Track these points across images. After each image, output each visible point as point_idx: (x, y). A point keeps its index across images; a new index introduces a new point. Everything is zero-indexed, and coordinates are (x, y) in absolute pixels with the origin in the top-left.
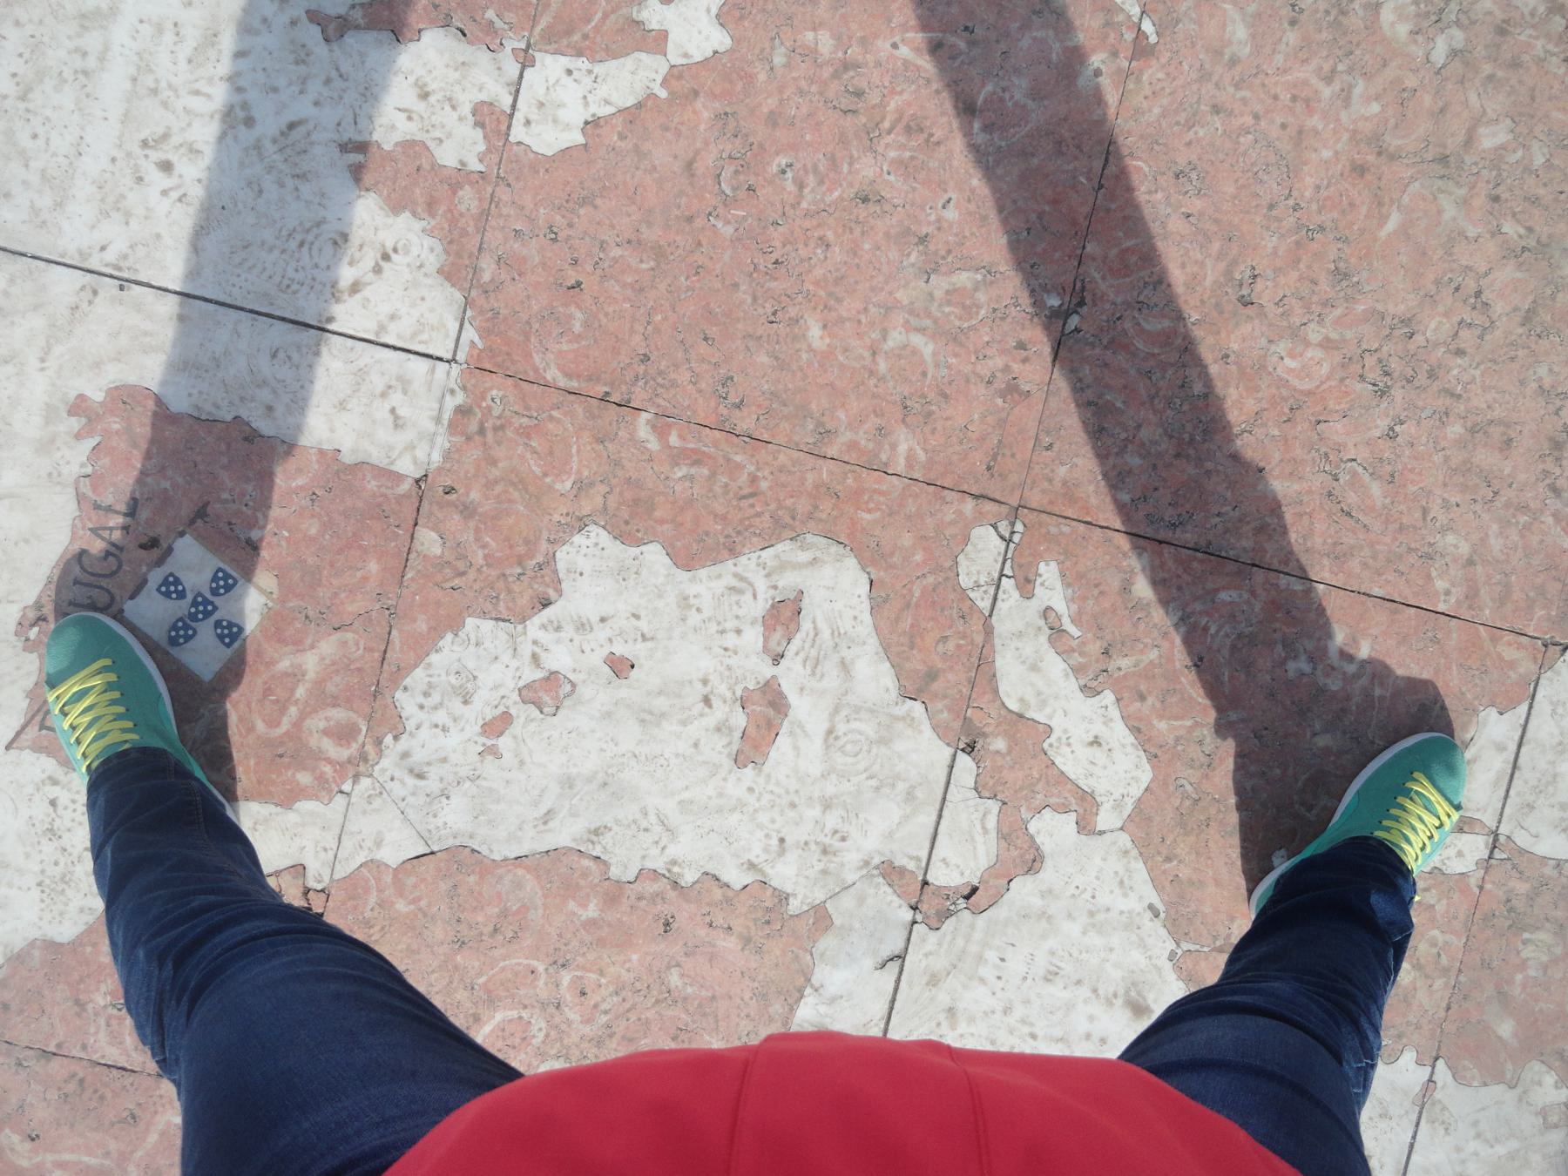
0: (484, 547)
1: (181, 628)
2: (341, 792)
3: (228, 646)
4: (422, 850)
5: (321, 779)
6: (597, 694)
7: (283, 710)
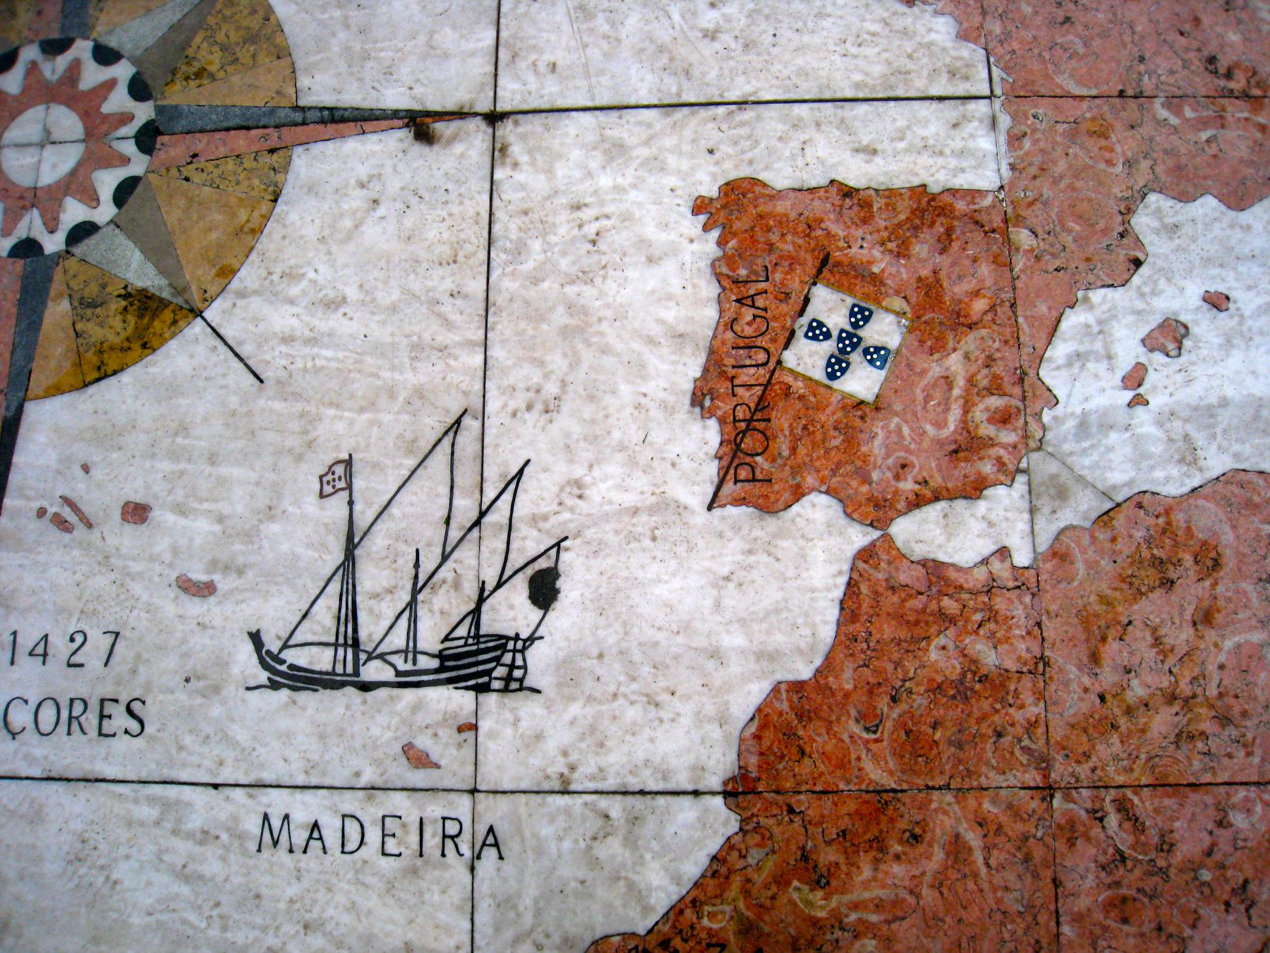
3: (881, 368)
4: (1108, 505)
5: (1000, 462)
6: (1205, 327)
7: (947, 410)
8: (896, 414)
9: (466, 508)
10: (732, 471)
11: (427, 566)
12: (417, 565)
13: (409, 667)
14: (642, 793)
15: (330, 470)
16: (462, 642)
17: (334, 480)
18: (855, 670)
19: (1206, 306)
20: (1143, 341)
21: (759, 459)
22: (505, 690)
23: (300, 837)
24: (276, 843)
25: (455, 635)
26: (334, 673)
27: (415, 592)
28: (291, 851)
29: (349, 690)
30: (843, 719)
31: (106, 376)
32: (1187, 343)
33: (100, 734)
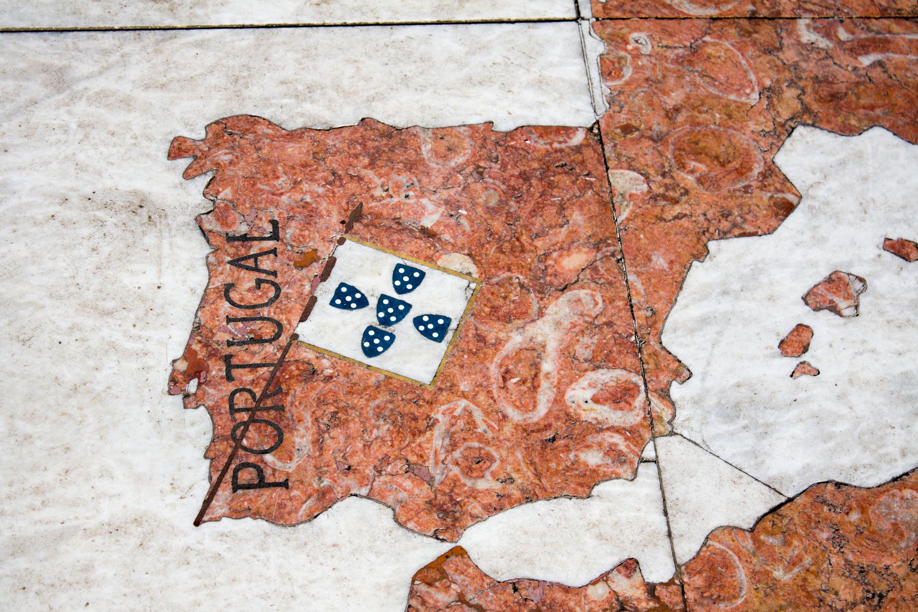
0: (692, 172)
1: (374, 337)
2: (643, 461)
3: (439, 339)
4: (776, 501)
8: (464, 396)
10: (229, 476)
19: (888, 256)
20: (805, 299)
21: (268, 458)
32: (864, 300)
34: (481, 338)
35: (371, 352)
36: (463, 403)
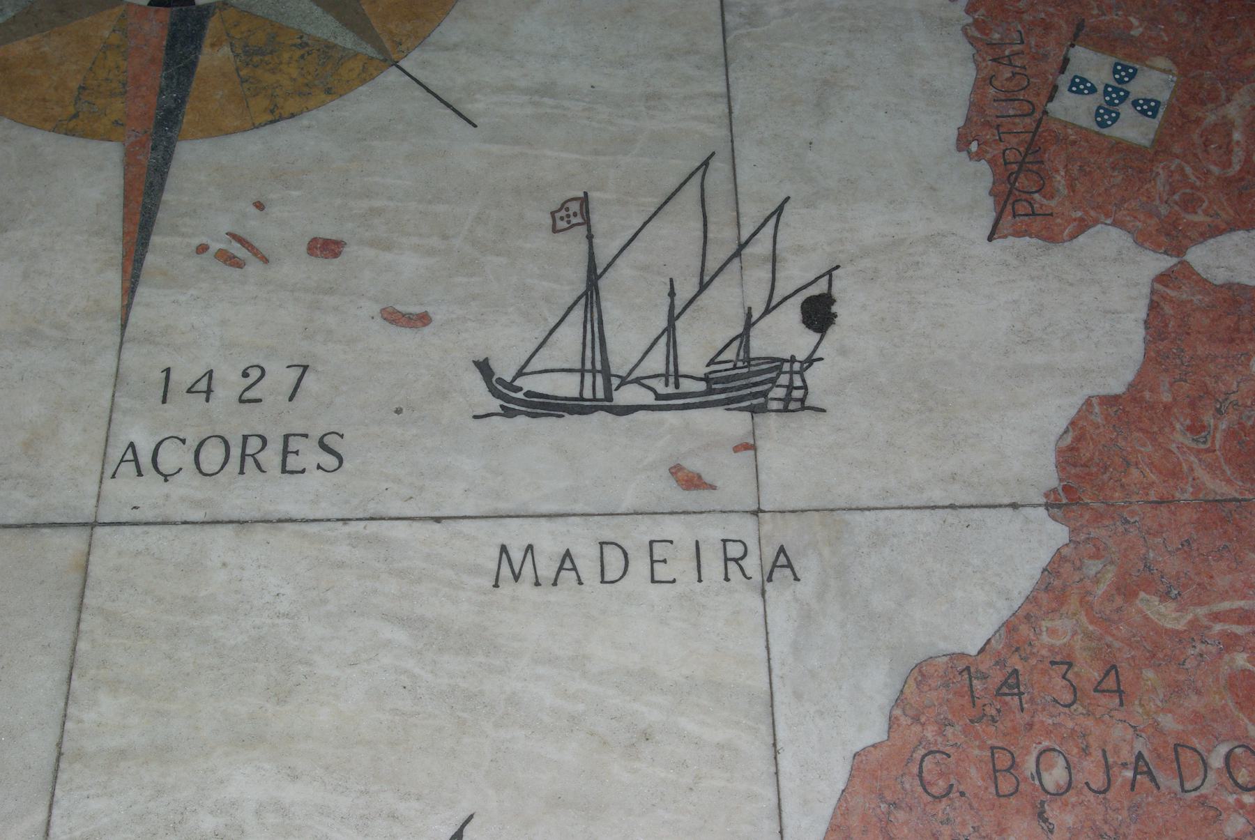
1: (1104, 114)
3: (1154, 116)
7: (1229, 151)
9: (723, 238)
10: (1009, 207)
11: (683, 295)
12: (672, 294)
13: (671, 390)
14: (952, 507)
15: (564, 206)
16: (730, 365)
17: (568, 216)
18: (1171, 385)
21: (1037, 196)
22: (786, 410)
23: (547, 569)
24: (516, 577)
25: (722, 358)
26: (582, 398)
27: (672, 319)
28: (537, 584)
29: (601, 415)
30: (1167, 430)
31: (281, 118)
33: (284, 471)
34: (1183, 115)
35: (1102, 124)
36: (1177, 161)
